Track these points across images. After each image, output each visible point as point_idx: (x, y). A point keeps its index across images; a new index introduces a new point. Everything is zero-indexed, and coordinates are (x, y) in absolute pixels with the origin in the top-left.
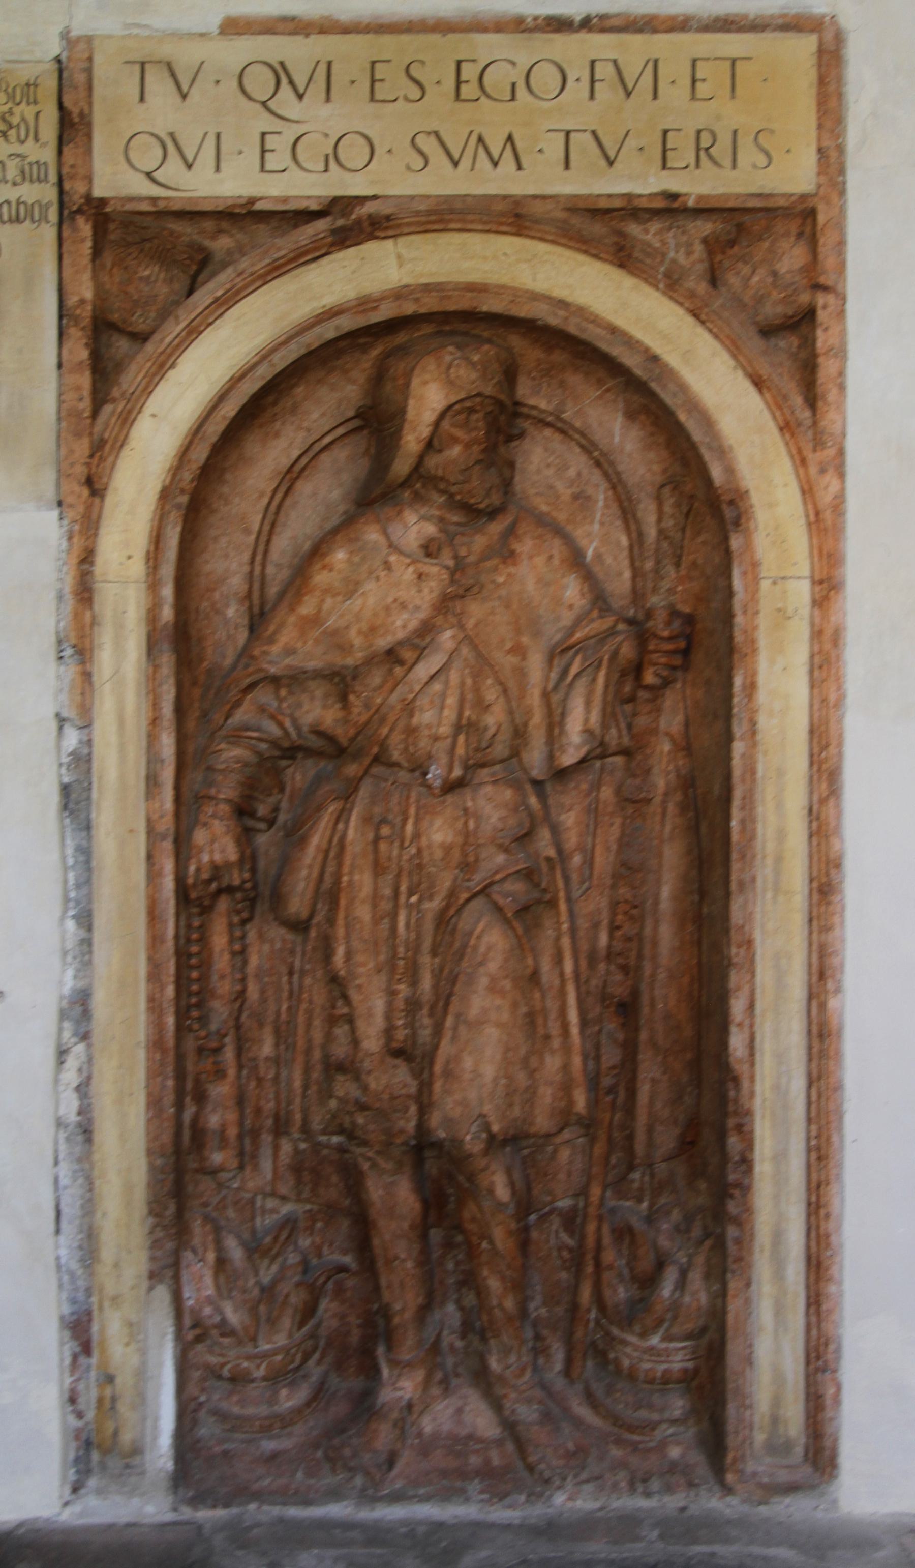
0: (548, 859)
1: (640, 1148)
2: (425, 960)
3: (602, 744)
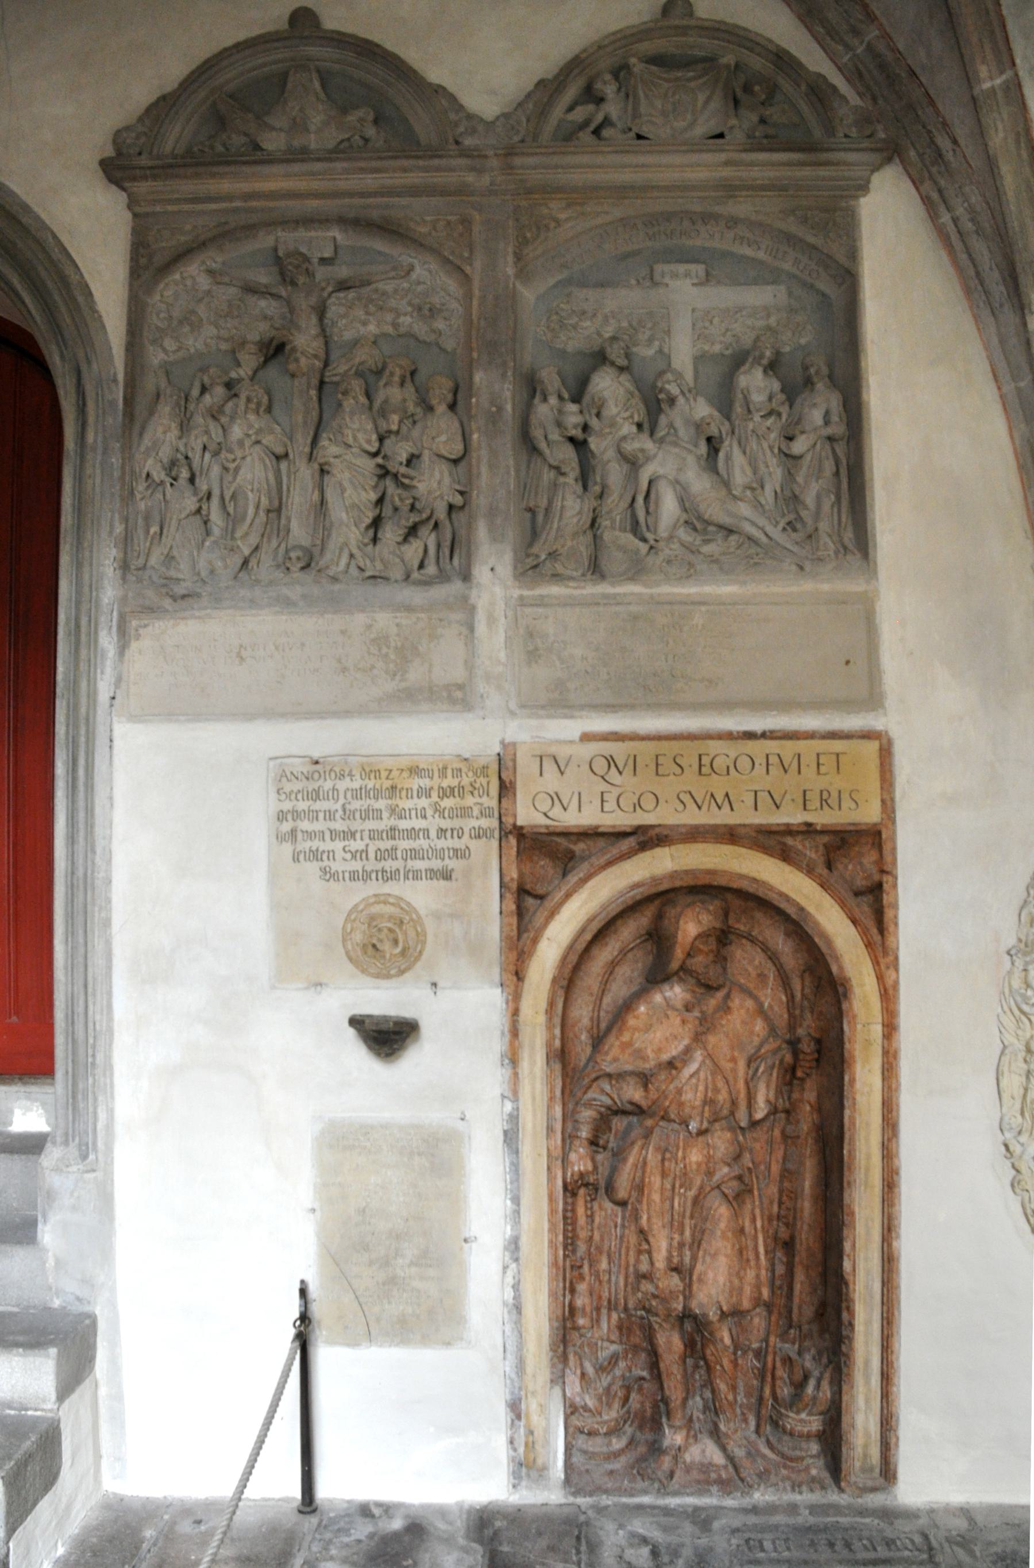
0: (749, 1169)
2: (687, 1221)
3: (776, 1108)
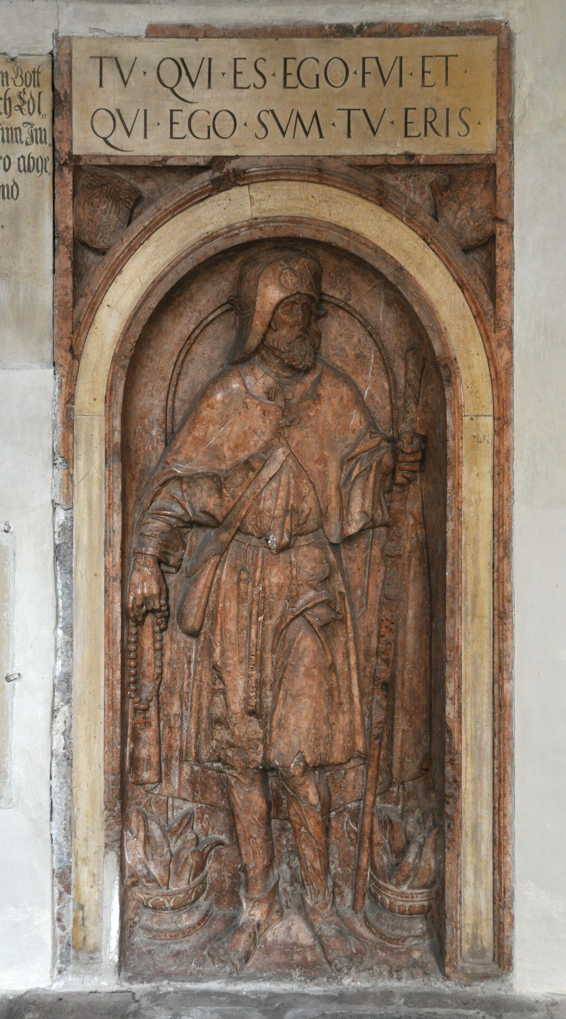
0: (341, 593)
1: (395, 772)
2: (268, 656)
3: (372, 520)
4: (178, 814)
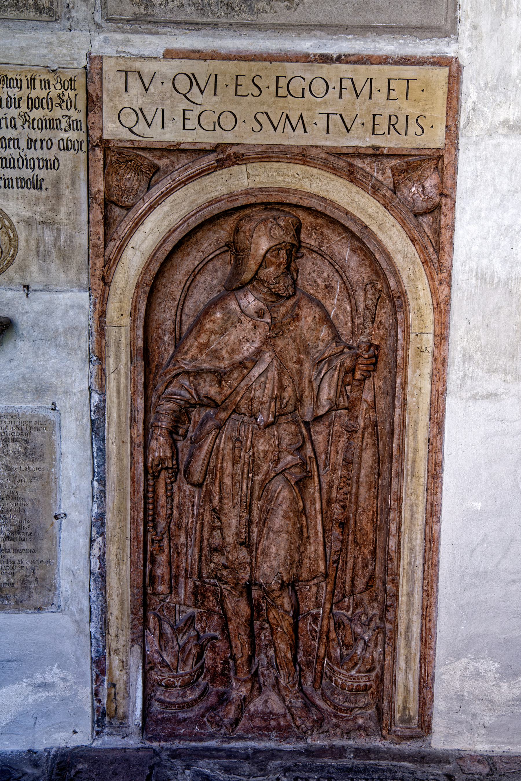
2: (255, 502)
4: (184, 616)
